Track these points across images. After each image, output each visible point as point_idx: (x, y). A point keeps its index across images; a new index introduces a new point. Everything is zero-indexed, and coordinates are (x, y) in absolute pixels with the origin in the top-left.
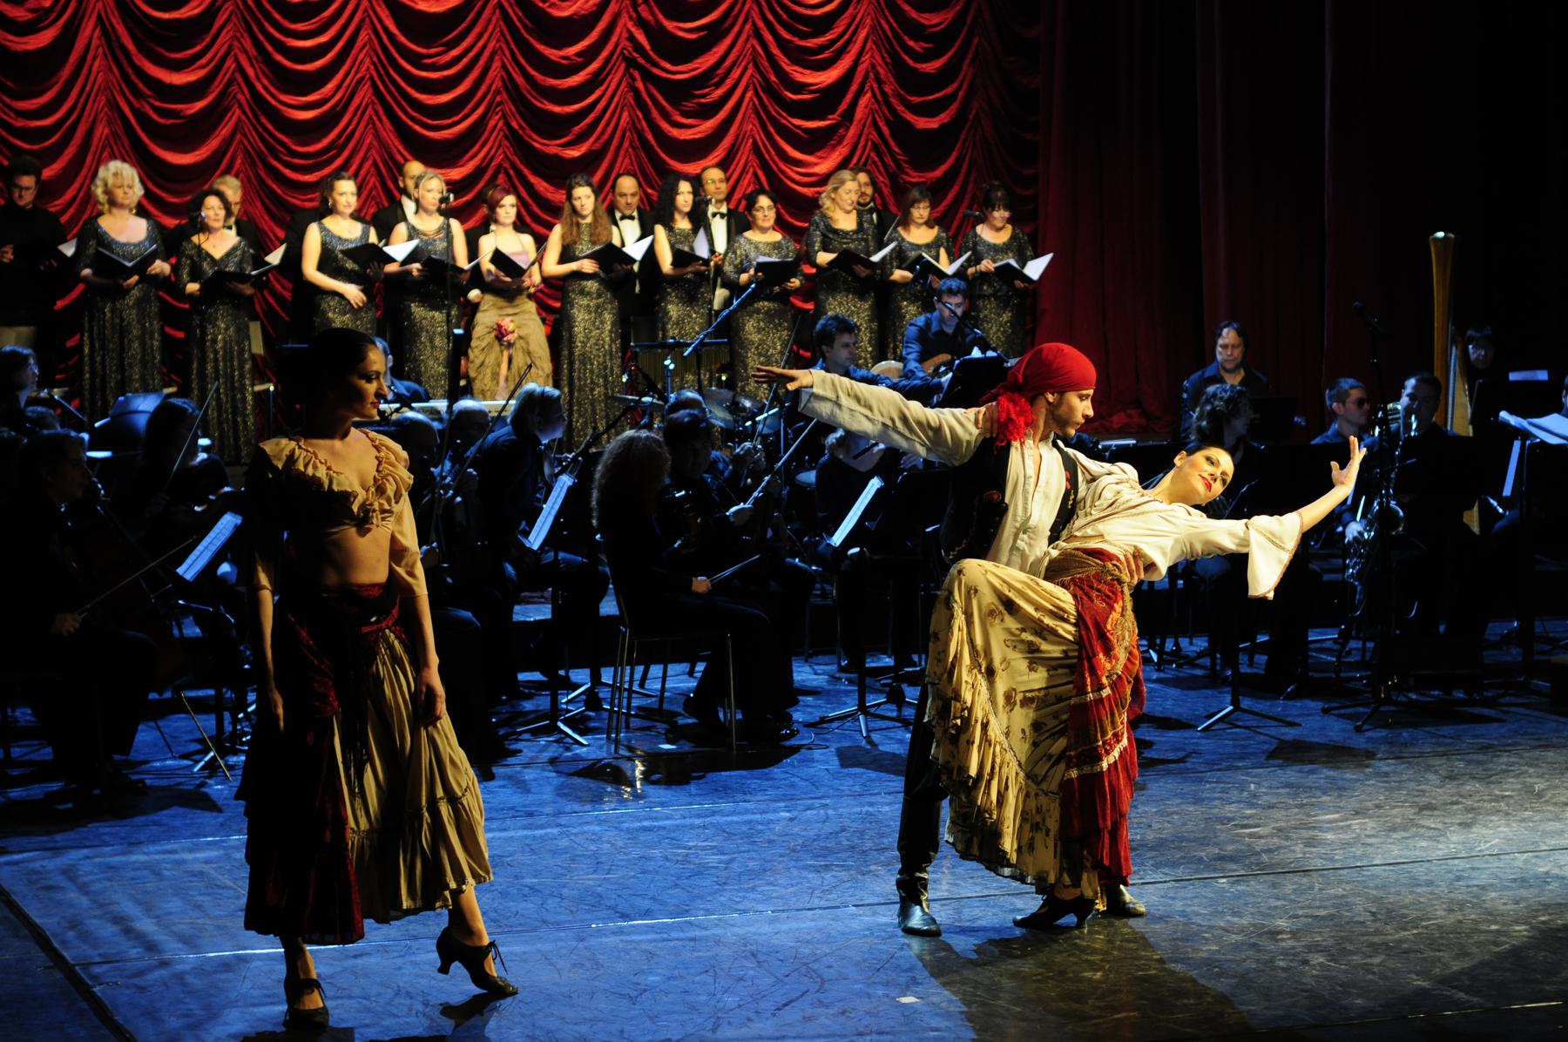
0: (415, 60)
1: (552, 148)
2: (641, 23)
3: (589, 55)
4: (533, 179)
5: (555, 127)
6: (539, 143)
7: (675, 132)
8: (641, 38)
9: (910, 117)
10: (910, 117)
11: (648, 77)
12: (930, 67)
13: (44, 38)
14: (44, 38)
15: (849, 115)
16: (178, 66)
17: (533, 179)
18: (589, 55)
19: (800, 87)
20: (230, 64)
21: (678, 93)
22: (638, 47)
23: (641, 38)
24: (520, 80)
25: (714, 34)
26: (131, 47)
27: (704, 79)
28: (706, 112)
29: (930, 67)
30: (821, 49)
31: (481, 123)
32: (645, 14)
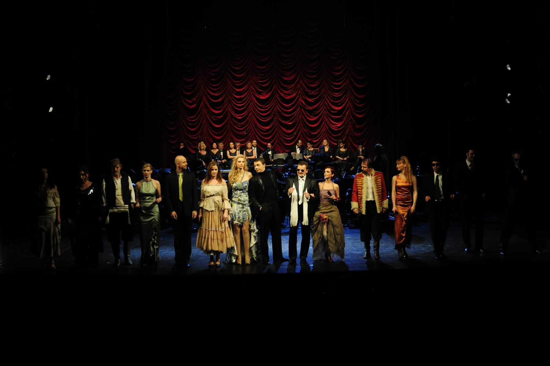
0: (260, 107)
1: (286, 123)
2: (303, 99)
3: (293, 106)
4: (283, 128)
5: (286, 119)
6: (283, 122)
7: (310, 119)
8: (303, 102)
9: (357, 115)
10: (357, 115)
11: (304, 109)
12: (360, 106)
13: (194, 106)
14: (194, 106)
15: (344, 116)
16: (218, 110)
17: (283, 128)
18: (293, 106)
19: (335, 110)
20: (227, 109)
21: (311, 112)
22: (302, 104)
23: (303, 102)
24: (280, 110)
25: (317, 101)
26: (209, 107)
27: (316, 109)
28: (316, 115)
29: (360, 106)
30: (339, 103)
31: (273, 118)
32: (304, 97)
